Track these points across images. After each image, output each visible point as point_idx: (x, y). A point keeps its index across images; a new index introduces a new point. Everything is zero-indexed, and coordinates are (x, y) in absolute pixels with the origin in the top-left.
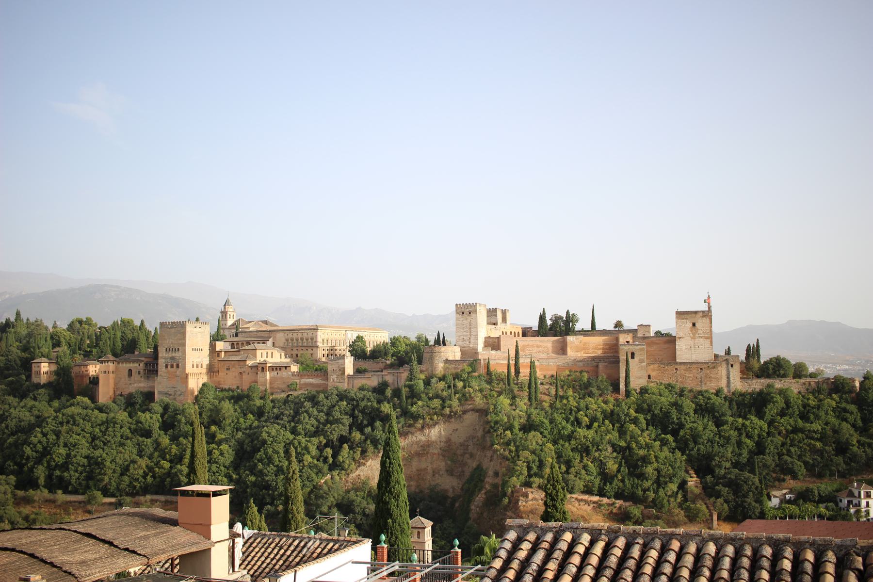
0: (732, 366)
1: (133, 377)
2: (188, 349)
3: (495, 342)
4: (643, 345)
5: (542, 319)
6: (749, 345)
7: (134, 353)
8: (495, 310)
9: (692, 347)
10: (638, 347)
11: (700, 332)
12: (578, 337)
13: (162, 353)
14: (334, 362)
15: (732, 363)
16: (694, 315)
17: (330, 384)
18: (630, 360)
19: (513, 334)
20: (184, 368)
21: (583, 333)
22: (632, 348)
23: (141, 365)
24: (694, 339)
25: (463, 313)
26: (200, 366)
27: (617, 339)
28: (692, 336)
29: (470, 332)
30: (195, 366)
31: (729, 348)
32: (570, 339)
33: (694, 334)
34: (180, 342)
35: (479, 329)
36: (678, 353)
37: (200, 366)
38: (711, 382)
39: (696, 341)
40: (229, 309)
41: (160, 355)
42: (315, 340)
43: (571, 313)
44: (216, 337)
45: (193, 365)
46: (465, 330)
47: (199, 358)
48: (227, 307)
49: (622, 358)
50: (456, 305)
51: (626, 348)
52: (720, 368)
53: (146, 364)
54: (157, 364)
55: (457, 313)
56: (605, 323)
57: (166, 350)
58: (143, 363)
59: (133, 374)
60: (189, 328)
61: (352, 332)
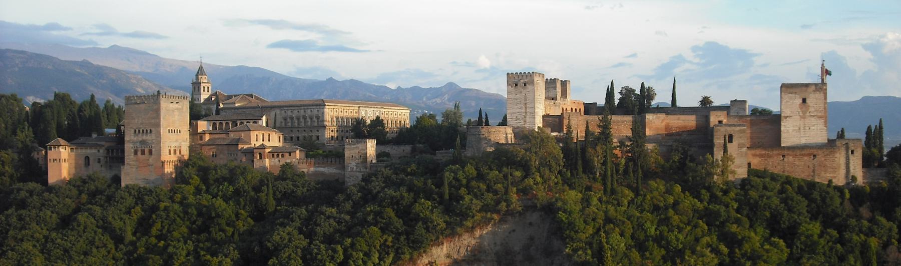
0: (852, 152)
1: (90, 167)
2: (163, 131)
3: (555, 121)
4: (744, 126)
5: (610, 94)
6: (869, 128)
7: (90, 135)
8: (554, 81)
9: (802, 128)
10: (738, 128)
11: (811, 109)
12: (659, 115)
13: (129, 137)
14: (353, 146)
15: (853, 148)
16: (804, 88)
17: (347, 174)
18: (729, 145)
19: (578, 111)
20: (159, 155)
21: (659, 110)
22: (730, 130)
23: (101, 151)
24: (804, 118)
25: (516, 85)
26: (178, 152)
27: (707, 118)
28: (801, 114)
29: (526, 108)
30: (172, 151)
31: (843, 131)
32: (649, 117)
33: (804, 113)
34: (153, 121)
35: (537, 105)
36: (783, 135)
37: (178, 152)
38: (826, 172)
39: (807, 121)
40: (204, 79)
41: (127, 138)
42: (321, 119)
43: (646, 86)
44: (195, 116)
45: (170, 151)
46: (519, 106)
47: (177, 141)
48: (200, 76)
49: (718, 141)
50: (508, 74)
51: (722, 129)
52: (837, 155)
53: (108, 150)
54: (123, 151)
55: (508, 84)
56: (689, 98)
57: (135, 130)
58: (104, 148)
59: (91, 163)
60: (164, 104)
61: (366, 109)
